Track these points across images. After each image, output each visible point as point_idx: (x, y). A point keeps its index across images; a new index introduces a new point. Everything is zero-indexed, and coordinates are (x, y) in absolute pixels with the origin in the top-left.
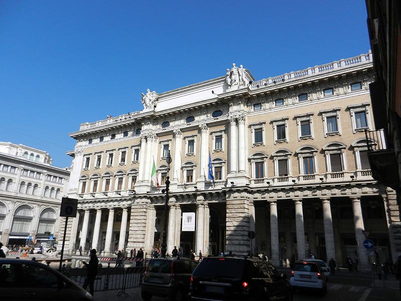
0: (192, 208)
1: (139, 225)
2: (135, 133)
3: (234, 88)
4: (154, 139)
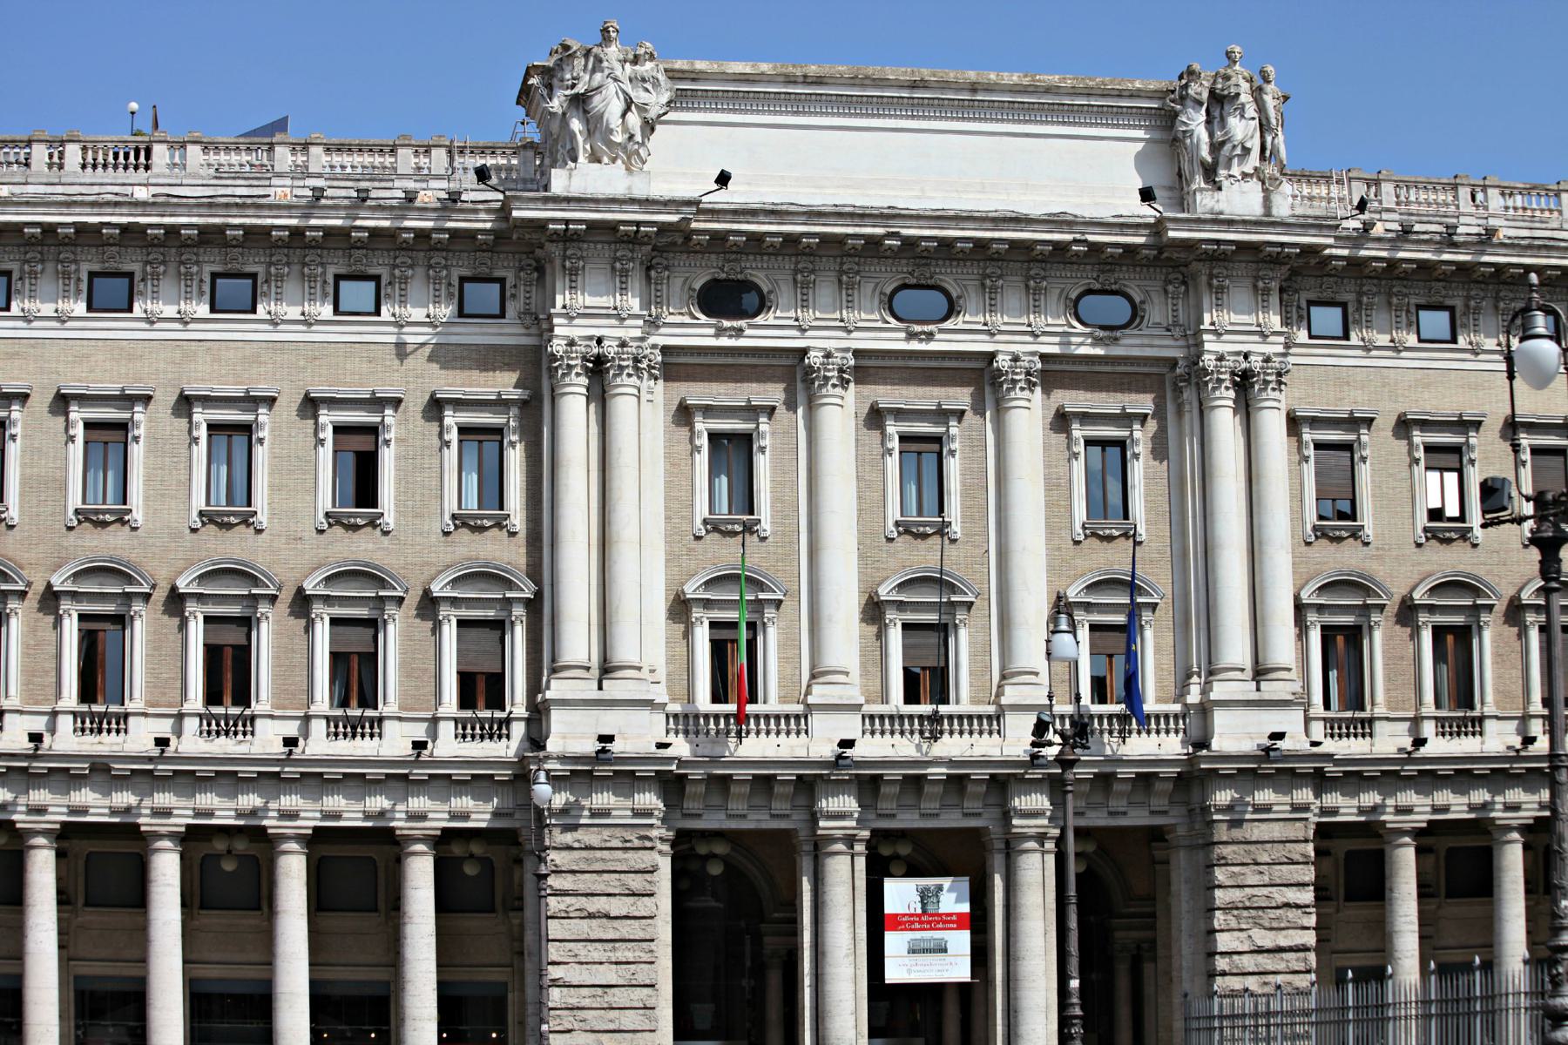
1: (624, 953)
3: (1239, 198)
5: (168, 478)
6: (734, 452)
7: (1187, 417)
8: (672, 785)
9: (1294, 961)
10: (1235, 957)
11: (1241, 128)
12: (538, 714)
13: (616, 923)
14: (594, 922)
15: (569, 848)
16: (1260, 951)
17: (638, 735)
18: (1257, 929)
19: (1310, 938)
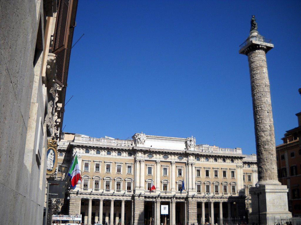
0: (168, 203)
5: (103, 169)
8: (145, 197)
9: (195, 213)
11: (192, 143)
12: (134, 191)
17: (143, 193)
18: (193, 210)
19: (196, 211)
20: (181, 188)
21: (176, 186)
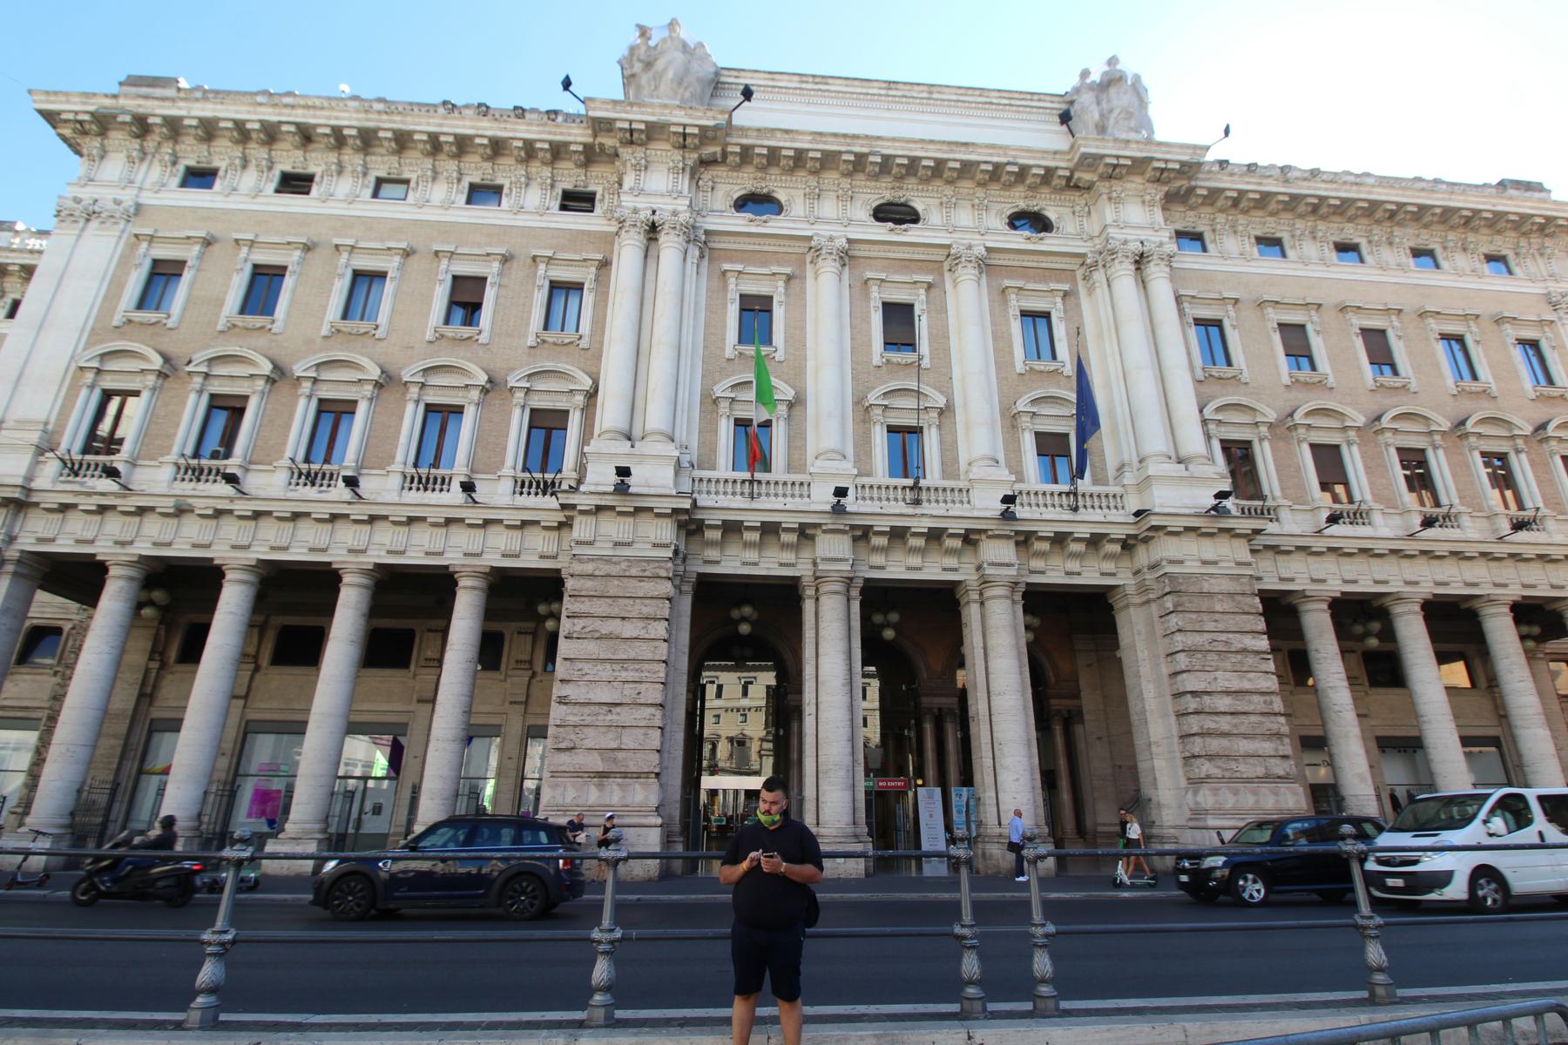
2: (557, 206)
4: (694, 252)
6: (756, 310)
7: (1098, 291)
8: (690, 524)
10: (1206, 698)
13: (623, 646)
14: (604, 643)
15: (591, 576)
16: (1227, 693)
20: (1067, 451)
21: (1013, 449)
